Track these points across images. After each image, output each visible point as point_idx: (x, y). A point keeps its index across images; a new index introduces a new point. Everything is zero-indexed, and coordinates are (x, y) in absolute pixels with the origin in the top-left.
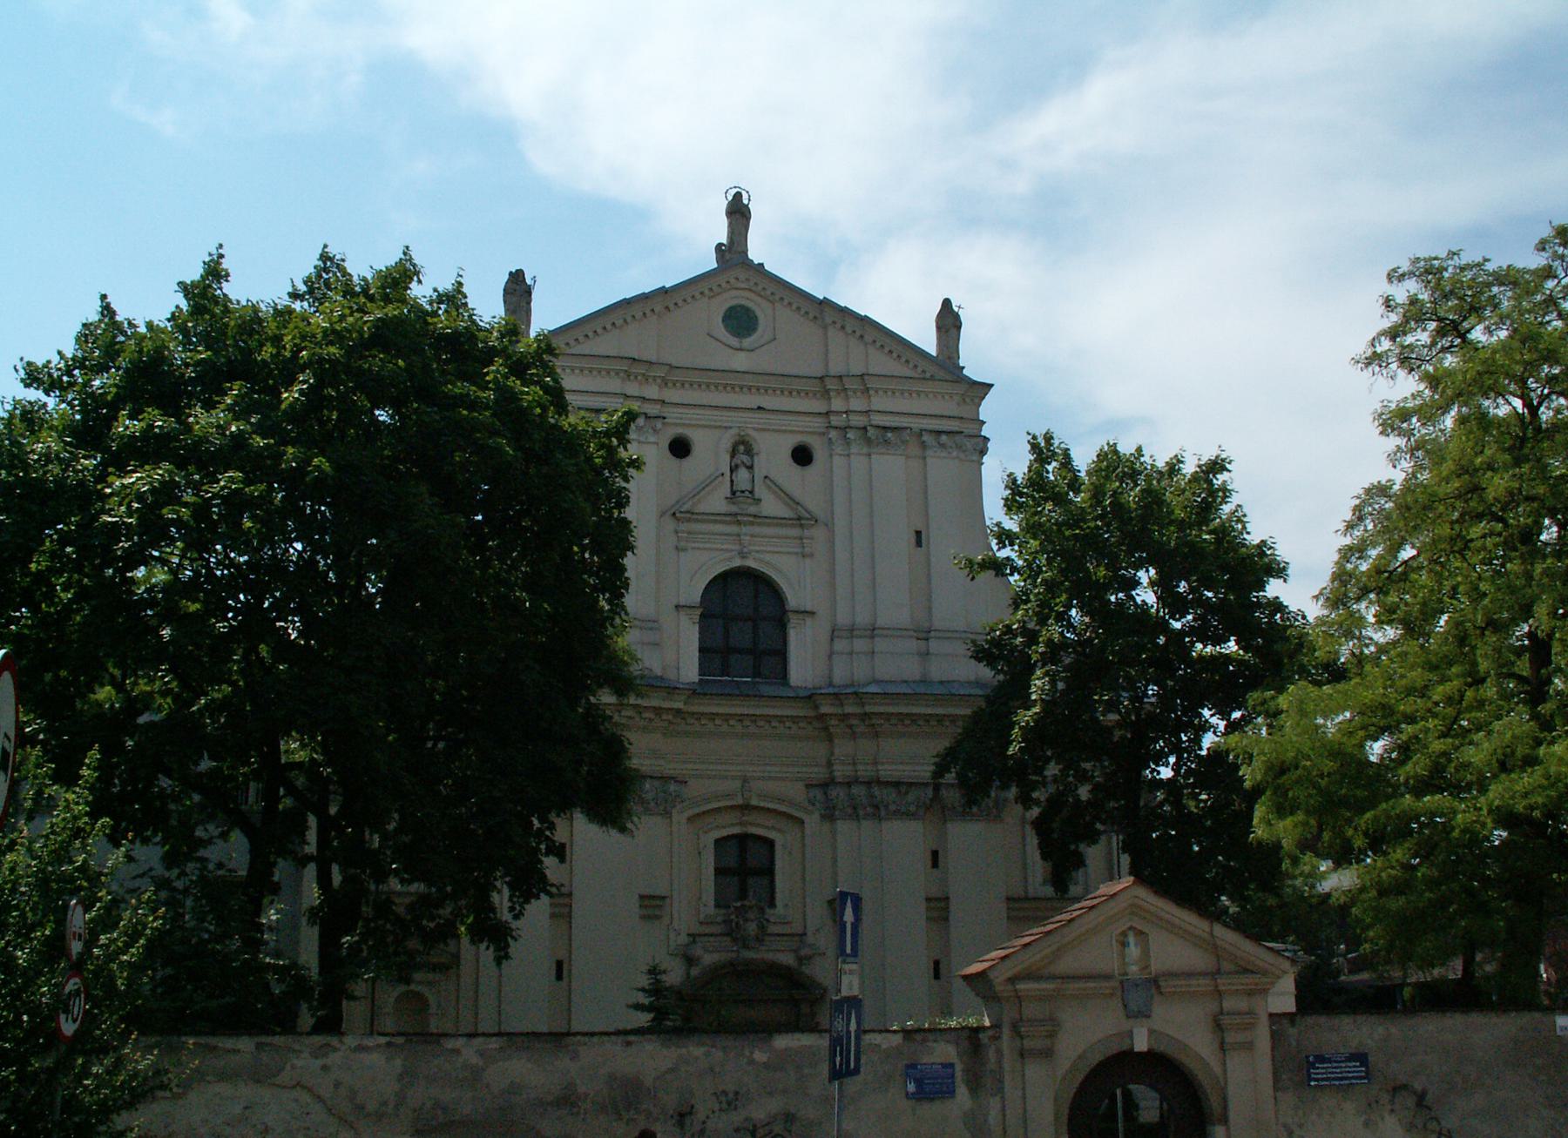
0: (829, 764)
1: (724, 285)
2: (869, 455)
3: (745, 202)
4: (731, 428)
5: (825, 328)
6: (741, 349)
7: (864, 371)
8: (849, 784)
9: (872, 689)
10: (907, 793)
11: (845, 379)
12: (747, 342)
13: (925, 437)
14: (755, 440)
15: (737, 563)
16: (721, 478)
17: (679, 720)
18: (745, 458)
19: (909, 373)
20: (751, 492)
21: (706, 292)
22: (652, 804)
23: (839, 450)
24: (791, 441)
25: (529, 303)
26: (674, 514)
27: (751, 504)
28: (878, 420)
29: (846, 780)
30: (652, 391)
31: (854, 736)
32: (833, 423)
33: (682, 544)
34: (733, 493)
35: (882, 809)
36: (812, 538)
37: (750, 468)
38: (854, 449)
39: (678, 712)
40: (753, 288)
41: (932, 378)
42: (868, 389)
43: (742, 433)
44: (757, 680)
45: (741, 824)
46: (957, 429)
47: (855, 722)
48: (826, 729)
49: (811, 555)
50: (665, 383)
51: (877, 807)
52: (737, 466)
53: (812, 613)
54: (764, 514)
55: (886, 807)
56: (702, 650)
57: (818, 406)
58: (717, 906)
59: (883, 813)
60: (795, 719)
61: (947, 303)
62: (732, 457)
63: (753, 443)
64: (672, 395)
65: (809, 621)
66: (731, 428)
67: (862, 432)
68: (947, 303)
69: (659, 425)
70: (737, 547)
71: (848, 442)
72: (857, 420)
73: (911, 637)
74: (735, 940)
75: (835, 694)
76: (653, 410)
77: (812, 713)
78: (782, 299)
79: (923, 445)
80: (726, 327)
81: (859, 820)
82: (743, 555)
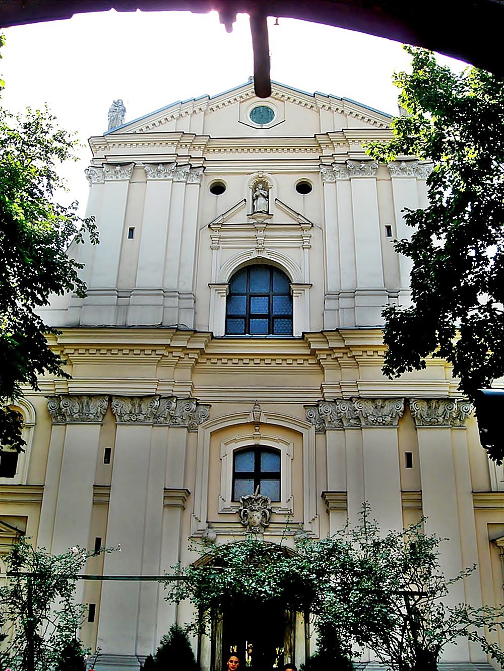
12: (266, 126)
15: (255, 255)
17: (204, 361)
20: (267, 213)
21: (238, 99)
24: (297, 179)
28: (353, 156)
30: (198, 153)
48: (319, 363)
52: (257, 197)
58: (233, 501)
63: (267, 181)
67: (344, 166)
74: (245, 526)
76: (195, 164)
82: (258, 250)
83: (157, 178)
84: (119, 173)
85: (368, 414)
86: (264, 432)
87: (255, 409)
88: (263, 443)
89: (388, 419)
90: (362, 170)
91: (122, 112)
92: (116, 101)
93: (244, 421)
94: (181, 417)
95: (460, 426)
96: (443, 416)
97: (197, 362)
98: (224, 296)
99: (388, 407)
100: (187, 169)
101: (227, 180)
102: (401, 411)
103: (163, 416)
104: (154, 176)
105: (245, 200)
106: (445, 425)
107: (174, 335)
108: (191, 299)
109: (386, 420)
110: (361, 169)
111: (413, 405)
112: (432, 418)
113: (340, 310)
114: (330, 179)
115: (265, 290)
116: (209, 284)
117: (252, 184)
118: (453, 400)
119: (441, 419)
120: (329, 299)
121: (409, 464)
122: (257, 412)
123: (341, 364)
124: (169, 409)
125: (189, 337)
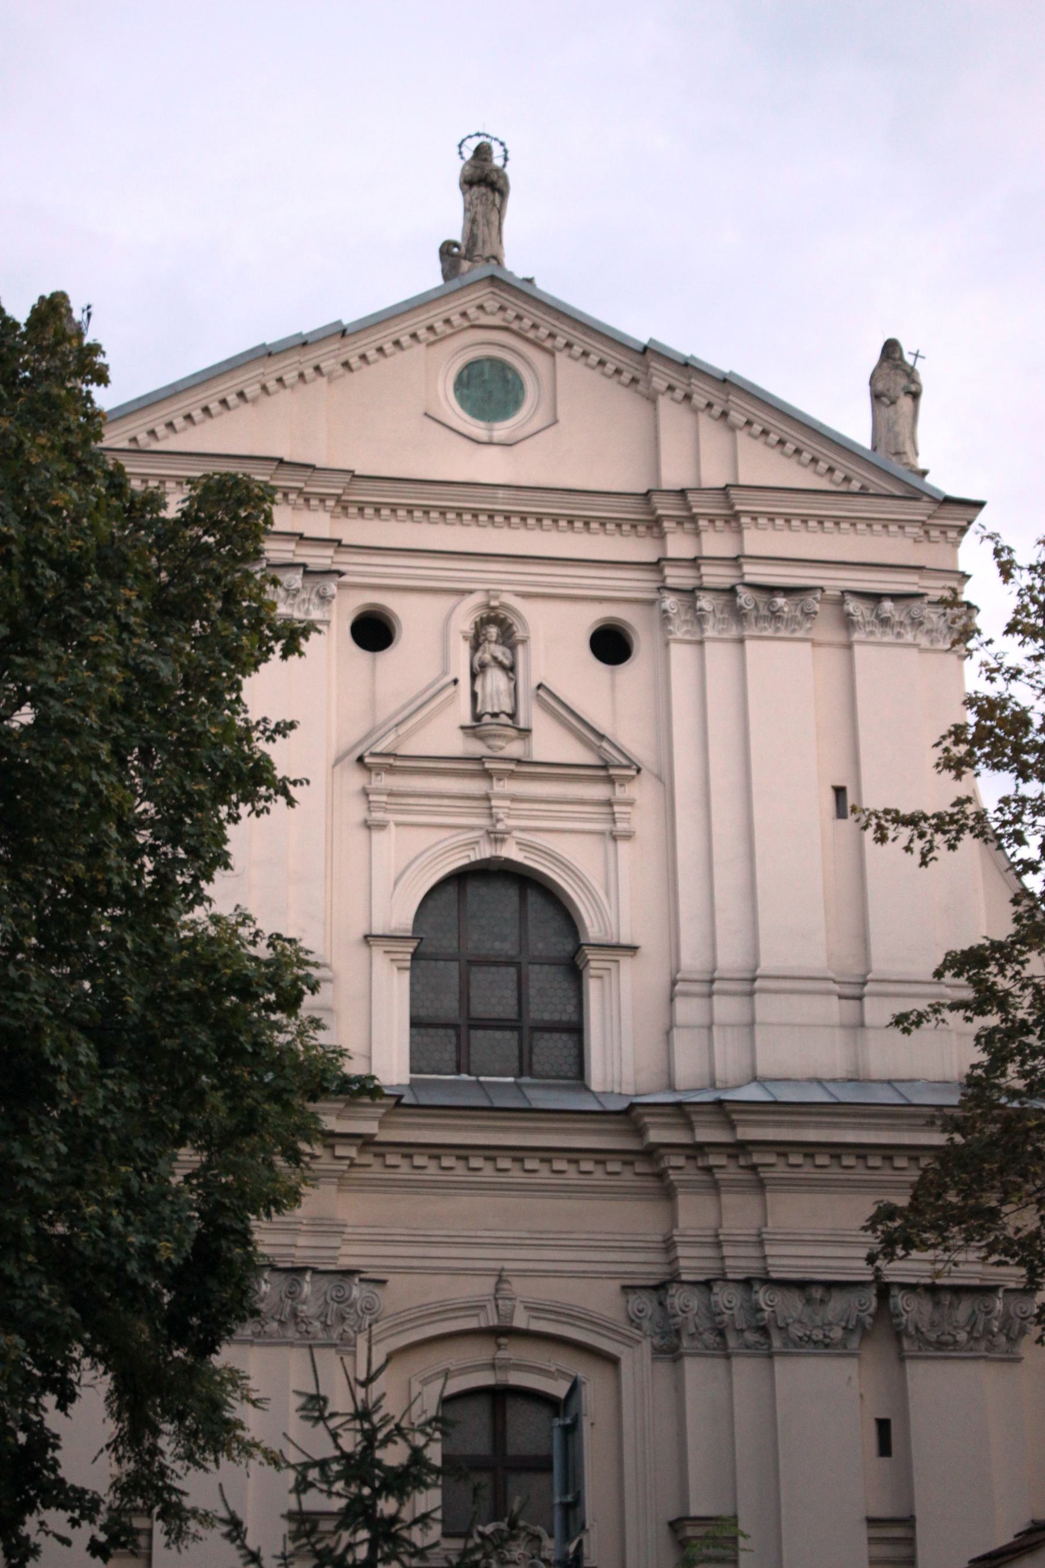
0: (669, 1245)
1: (456, 319)
2: (741, 641)
3: (498, 162)
4: (471, 592)
5: (652, 399)
6: (490, 443)
7: (731, 482)
8: (707, 1285)
9: (753, 1093)
10: (822, 1301)
11: (691, 497)
12: (502, 430)
13: (852, 605)
14: (519, 616)
15: (485, 851)
16: (452, 689)
17: (368, 1159)
18: (500, 652)
19: (823, 484)
20: (512, 716)
21: (422, 333)
22: (317, 1324)
23: (679, 630)
26: (360, 759)
27: (510, 739)
28: (755, 573)
29: (701, 1278)
31: (715, 1187)
32: (670, 582)
33: (378, 816)
34: (477, 717)
35: (775, 1334)
36: (630, 803)
37: (510, 670)
38: (710, 632)
39: (366, 1142)
40: (515, 326)
41: (863, 493)
42: (736, 516)
43: (494, 603)
44: (526, 1080)
45: (493, 1366)
46: (914, 589)
47: (713, 1160)
48: (661, 1175)
49: (628, 836)
50: (343, 506)
52: (483, 666)
54: (537, 757)
57: (642, 550)
59: (777, 1343)
60: (600, 1155)
61: (891, 349)
63: (512, 619)
65: (626, 963)
66: (471, 592)
67: (724, 598)
68: (891, 349)
70: (484, 822)
71: (699, 618)
72: (716, 576)
73: (828, 993)
75: (678, 1105)
76: (319, 558)
77: (629, 1144)
79: (848, 623)
80: (462, 400)
81: (728, 1357)
85: (790, 1321)
88: (516, 1379)
89: (837, 1333)
90: (775, 616)
92: (48, 296)
93: (472, 1324)
94: (322, 1319)
95: (1007, 1352)
96: (968, 1329)
97: (352, 1165)
99: (837, 1305)
102: (870, 1315)
103: (278, 1317)
106: (971, 1350)
109: (832, 1335)
110: (773, 613)
111: (899, 1300)
112: (943, 1334)
113: (715, 1029)
114: (688, 632)
115: (508, 947)
117: (467, 625)
118: (991, 1290)
119: (962, 1336)
120: (686, 994)
121: (885, 1448)
122: (508, 1302)
123: (721, 1183)
124: (293, 1299)
125: (341, 1106)
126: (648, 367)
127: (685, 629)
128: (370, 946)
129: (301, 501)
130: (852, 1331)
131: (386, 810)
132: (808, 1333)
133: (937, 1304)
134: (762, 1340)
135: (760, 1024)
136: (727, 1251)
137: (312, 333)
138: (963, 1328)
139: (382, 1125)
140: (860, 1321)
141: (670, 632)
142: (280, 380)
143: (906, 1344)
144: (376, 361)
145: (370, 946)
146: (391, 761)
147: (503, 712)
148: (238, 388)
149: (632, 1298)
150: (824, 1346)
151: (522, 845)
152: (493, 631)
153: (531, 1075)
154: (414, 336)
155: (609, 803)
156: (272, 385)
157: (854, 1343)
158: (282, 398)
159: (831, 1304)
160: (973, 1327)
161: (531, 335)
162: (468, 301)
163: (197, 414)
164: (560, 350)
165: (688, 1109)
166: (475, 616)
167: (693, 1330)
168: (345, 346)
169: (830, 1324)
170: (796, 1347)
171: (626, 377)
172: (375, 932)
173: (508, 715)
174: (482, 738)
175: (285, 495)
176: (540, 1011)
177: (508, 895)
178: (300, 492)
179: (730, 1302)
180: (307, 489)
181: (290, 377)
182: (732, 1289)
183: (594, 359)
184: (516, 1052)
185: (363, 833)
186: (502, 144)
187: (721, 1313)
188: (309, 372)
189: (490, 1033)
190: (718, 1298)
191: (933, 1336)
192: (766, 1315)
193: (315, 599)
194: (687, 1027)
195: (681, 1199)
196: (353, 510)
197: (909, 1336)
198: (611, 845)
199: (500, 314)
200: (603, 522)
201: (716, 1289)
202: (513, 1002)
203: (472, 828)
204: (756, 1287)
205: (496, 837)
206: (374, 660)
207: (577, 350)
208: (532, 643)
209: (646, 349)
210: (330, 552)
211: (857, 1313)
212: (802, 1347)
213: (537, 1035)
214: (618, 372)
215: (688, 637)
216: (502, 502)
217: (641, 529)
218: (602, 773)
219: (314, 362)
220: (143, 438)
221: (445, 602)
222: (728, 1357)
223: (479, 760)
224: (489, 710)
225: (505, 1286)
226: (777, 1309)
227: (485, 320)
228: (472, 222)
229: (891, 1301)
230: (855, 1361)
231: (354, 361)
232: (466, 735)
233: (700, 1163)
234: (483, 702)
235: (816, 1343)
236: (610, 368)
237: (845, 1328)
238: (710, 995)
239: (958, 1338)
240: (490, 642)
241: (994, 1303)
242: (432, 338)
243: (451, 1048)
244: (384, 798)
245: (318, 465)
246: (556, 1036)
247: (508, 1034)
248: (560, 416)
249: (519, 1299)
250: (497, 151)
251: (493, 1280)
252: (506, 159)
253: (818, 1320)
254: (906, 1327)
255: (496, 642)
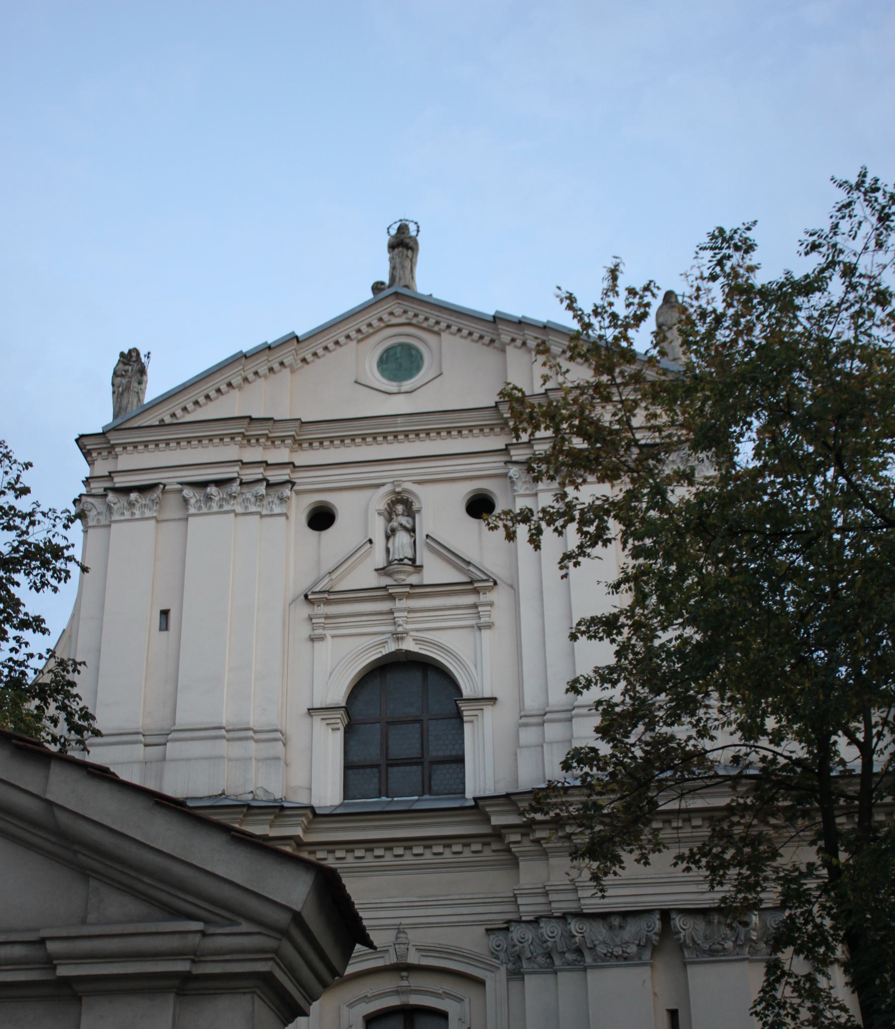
1: (375, 323)
3: (413, 233)
4: (383, 485)
6: (399, 393)
8: (536, 921)
12: (407, 385)
15: (392, 647)
16: (369, 545)
18: (404, 520)
20: (413, 560)
21: (353, 334)
24: (463, 492)
25: (140, 383)
27: (409, 574)
33: (319, 632)
34: (390, 563)
35: (586, 953)
36: (491, 604)
37: (412, 531)
40: (414, 321)
43: (398, 489)
44: (427, 797)
45: (397, 992)
47: (539, 834)
48: (508, 850)
49: (489, 626)
50: (298, 443)
51: (579, 951)
53: (493, 700)
54: (425, 583)
55: (592, 949)
56: (349, 767)
59: (589, 960)
60: (466, 839)
62: (390, 520)
63: (411, 498)
64: (302, 458)
66: (383, 485)
69: (287, 491)
70: (391, 628)
76: (275, 476)
78: (449, 327)
81: (555, 972)
83: (205, 510)
84: (138, 505)
86: (417, 981)
87: (400, 941)
89: (633, 949)
91: (138, 375)
92: (126, 352)
96: (733, 939)
98: (338, 729)
99: (632, 929)
100: (262, 489)
101: (339, 502)
102: (655, 934)
104: (200, 508)
105: (370, 541)
107: (245, 815)
108: (276, 740)
109: (628, 951)
111: (678, 921)
113: (545, 746)
114: (527, 489)
116: (309, 710)
117: (382, 506)
119: (729, 945)
120: (526, 725)
122: (402, 946)
125: (272, 817)
126: (497, 329)
127: (525, 487)
128: (312, 716)
129: (269, 443)
130: (643, 946)
131: (324, 628)
132: (610, 950)
133: (709, 923)
134: (579, 958)
135: (577, 738)
136: (553, 897)
137: (275, 342)
138: (729, 939)
139: (306, 830)
140: (648, 939)
141: (515, 491)
142: (256, 373)
143: (686, 953)
144: (324, 355)
145: (312, 716)
146: (326, 596)
147: (406, 558)
148: (227, 380)
149: (492, 937)
150: (625, 959)
151: (416, 640)
152: (400, 508)
153: (430, 794)
154: (348, 337)
155: (475, 606)
156: (251, 377)
157: (647, 956)
158: (260, 383)
159: (628, 928)
160: (737, 938)
161: (425, 325)
162: (382, 311)
163: (202, 400)
164: (444, 331)
165: (514, 798)
166: (387, 500)
167: (530, 955)
168: (302, 348)
169: (627, 943)
170: (603, 961)
171: (487, 340)
172: (316, 706)
173: (410, 559)
174: (389, 575)
175: (258, 440)
176: (436, 750)
177: (416, 677)
178: (268, 438)
179: (552, 933)
180: (270, 435)
181: (263, 370)
182: (554, 923)
183: (465, 332)
184: (420, 779)
185: (309, 644)
186: (416, 223)
187: (546, 941)
188: (276, 366)
189: (402, 768)
190: (543, 930)
191: (706, 946)
192: (577, 939)
193: (277, 501)
194: (527, 747)
195: (521, 864)
196: (306, 445)
197: (688, 948)
198: (477, 633)
199: (405, 316)
200: (470, 429)
201: (542, 925)
202: (418, 746)
203: (383, 633)
204: (569, 920)
205: (398, 637)
206: (320, 535)
207: (454, 329)
208: (423, 511)
209: (494, 317)
210: (288, 471)
211: (645, 933)
212: (608, 961)
213: (435, 767)
214: (481, 337)
215: (528, 492)
216: (401, 426)
217: (497, 430)
218: (470, 587)
219: (280, 359)
220: (168, 420)
221: (367, 493)
222: (555, 972)
223: (385, 588)
224: (397, 557)
225: (402, 935)
226: (585, 934)
227: (394, 321)
228: (393, 268)
229: (672, 923)
230: (648, 968)
231: (309, 357)
232: (380, 575)
233: (531, 838)
234: (394, 554)
235: (617, 957)
236: (476, 336)
237: (639, 945)
238: (542, 724)
239: (726, 946)
240: (397, 515)
241: (751, 918)
242: (360, 336)
243: (376, 780)
244: (322, 620)
245: (276, 418)
246: (447, 766)
247: (414, 768)
248: (444, 371)
249: (411, 943)
250: (412, 228)
251: (394, 932)
252: (418, 231)
253: (618, 940)
254: (685, 940)
255: (403, 515)
